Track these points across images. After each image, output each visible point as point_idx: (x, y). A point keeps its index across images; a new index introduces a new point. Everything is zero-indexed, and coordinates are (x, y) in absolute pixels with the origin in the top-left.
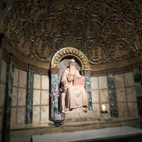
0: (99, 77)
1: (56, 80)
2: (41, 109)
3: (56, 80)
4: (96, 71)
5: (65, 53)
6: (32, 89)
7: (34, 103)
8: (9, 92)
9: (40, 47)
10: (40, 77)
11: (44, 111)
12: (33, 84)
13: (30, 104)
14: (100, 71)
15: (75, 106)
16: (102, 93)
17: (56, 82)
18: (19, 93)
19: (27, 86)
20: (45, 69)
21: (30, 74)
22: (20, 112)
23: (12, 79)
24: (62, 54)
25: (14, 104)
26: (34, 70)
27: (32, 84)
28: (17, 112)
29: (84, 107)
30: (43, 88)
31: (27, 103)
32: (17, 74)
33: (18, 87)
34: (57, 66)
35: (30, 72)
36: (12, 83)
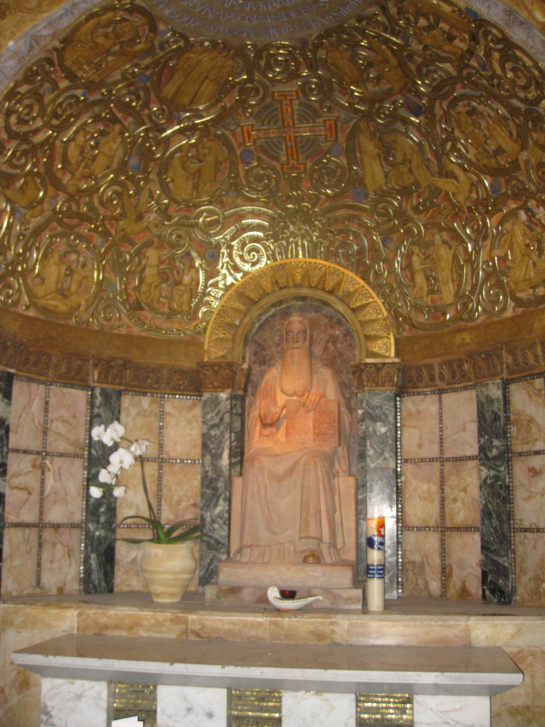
0: (444, 396)
1: (222, 419)
3: (222, 419)
13: (102, 519)
14: (449, 363)
16: (452, 480)
17: (222, 428)
20: (181, 372)
22: (55, 545)
28: (40, 545)
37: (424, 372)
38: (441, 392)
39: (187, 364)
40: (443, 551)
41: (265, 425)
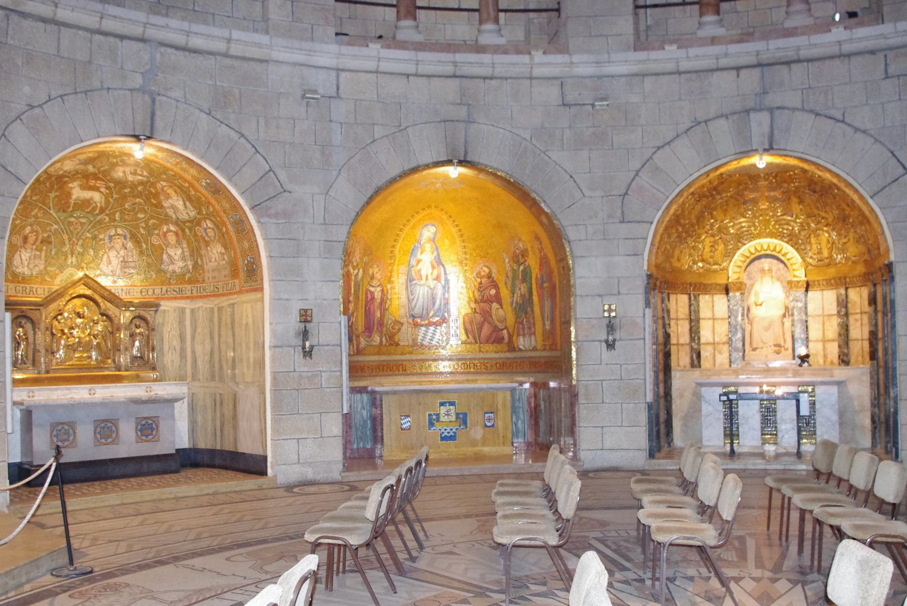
0: (824, 292)
2: (714, 349)
4: (818, 281)
5: (753, 251)
6: (698, 320)
7: (703, 340)
8: (667, 327)
9: (707, 249)
10: (711, 299)
11: (720, 353)
12: (699, 311)
14: (826, 280)
15: (761, 345)
16: (827, 323)
18: (679, 326)
19: (690, 315)
20: (720, 285)
21: (693, 298)
23: (668, 311)
24: (748, 255)
25: (673, 340)
26: (699, 289)
27: (697, 312)
29: (775, 345)
30: (717, 315)
31: (692, 339)
32: (674, 301)
33: (677, 319)
34: (739, 278)
35: (692, 295)
36: (669, 315)
37: (816, 283)
38: (823, 290)
39: (723, 281)
40: (824, 349)
41: (756, 305)
